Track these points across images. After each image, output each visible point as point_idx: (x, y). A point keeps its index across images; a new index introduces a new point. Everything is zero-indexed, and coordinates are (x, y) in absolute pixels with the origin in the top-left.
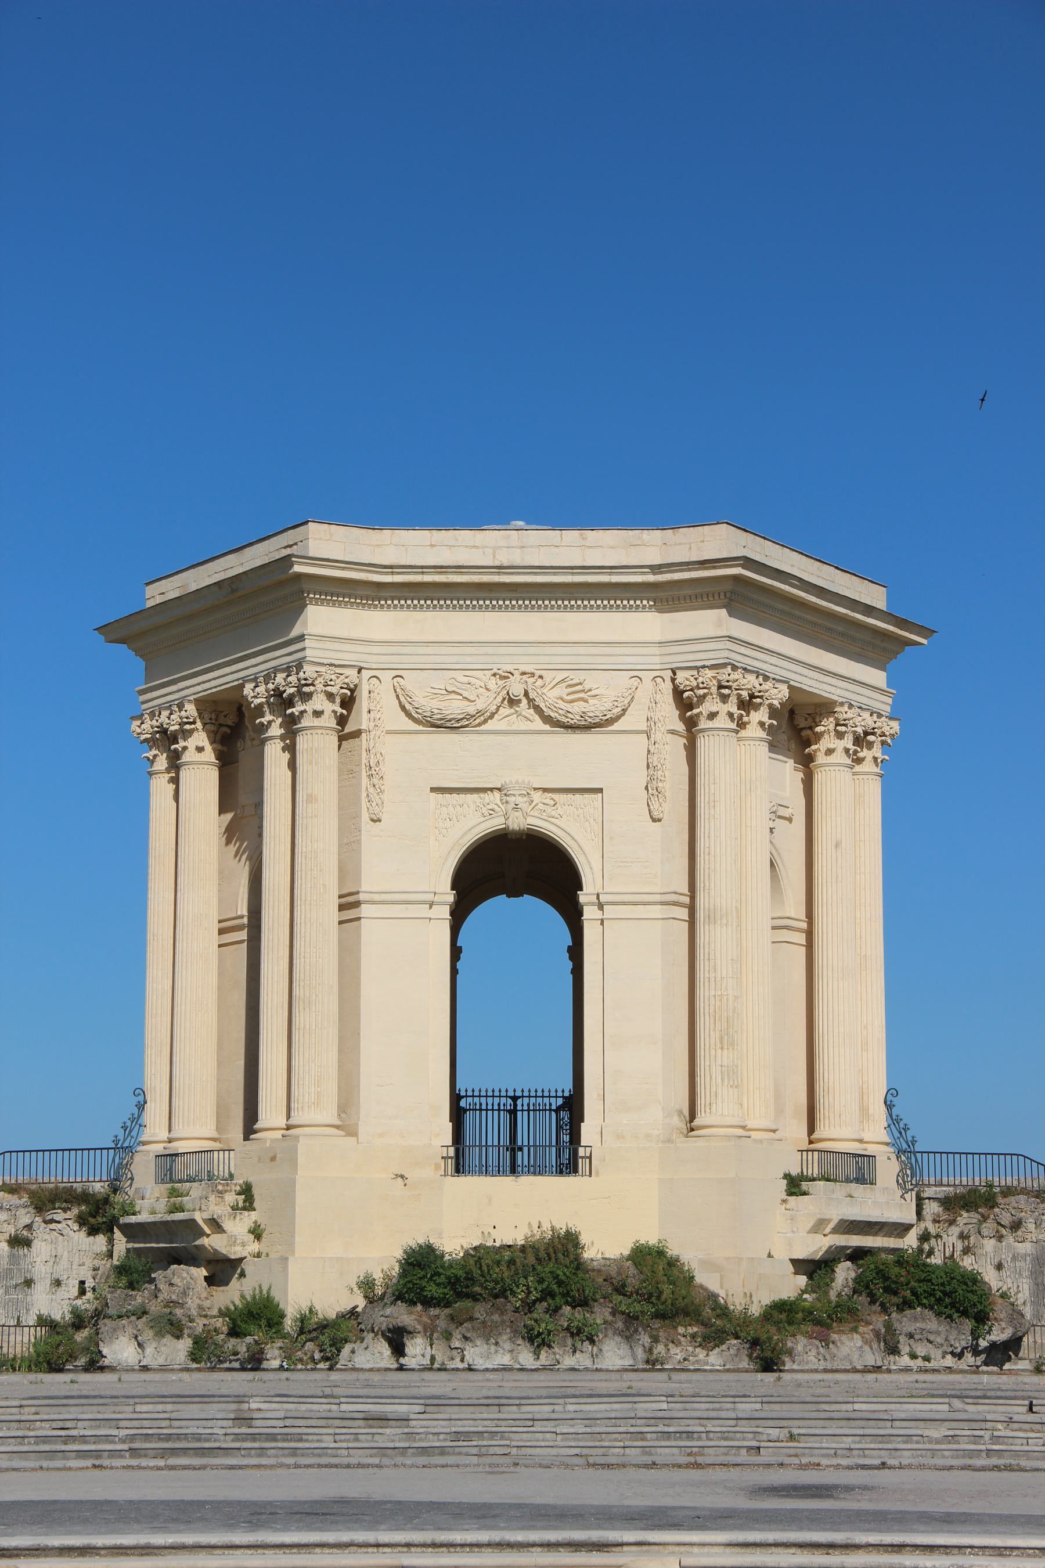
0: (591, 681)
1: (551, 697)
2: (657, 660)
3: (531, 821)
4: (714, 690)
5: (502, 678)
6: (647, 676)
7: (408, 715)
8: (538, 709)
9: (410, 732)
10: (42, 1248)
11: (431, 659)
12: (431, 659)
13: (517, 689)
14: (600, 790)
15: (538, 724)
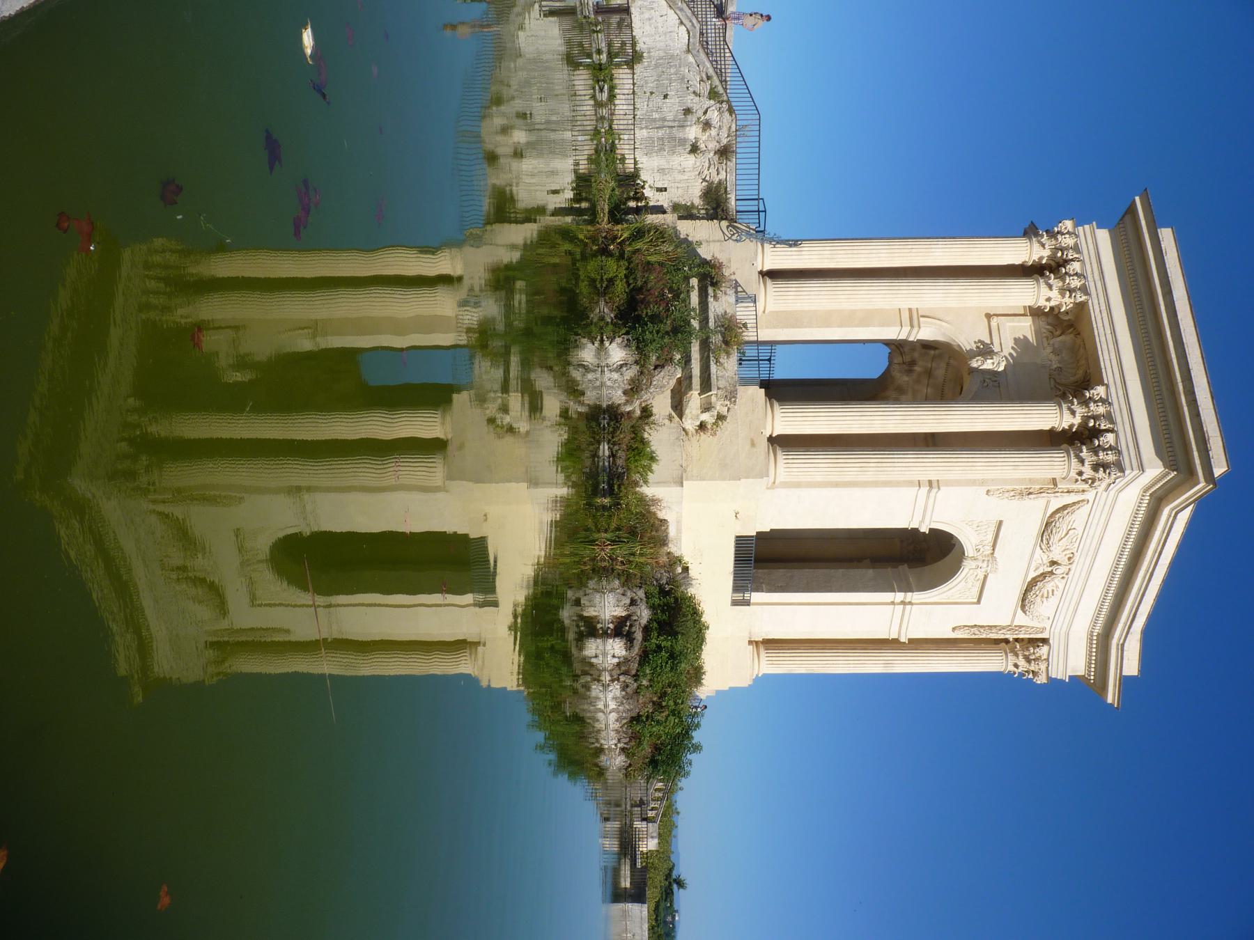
0: (1053, 601)
1: (1049, 585)
2: (1057, 631)
3: (966, 570)
4: (1032, 668)
5: (1069, 559)
6: (1047, 625)
7: (1058, 511)
8: (1043, 576)
9: (1045, 513)
10: (690, 161)
11: (1095, 522)
12: (1095, 522)
13: (1059, 571)
14: (979, 602)
15: (1032, 575)
